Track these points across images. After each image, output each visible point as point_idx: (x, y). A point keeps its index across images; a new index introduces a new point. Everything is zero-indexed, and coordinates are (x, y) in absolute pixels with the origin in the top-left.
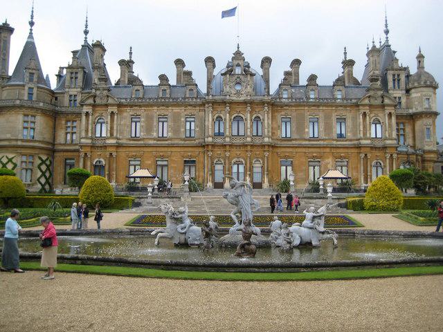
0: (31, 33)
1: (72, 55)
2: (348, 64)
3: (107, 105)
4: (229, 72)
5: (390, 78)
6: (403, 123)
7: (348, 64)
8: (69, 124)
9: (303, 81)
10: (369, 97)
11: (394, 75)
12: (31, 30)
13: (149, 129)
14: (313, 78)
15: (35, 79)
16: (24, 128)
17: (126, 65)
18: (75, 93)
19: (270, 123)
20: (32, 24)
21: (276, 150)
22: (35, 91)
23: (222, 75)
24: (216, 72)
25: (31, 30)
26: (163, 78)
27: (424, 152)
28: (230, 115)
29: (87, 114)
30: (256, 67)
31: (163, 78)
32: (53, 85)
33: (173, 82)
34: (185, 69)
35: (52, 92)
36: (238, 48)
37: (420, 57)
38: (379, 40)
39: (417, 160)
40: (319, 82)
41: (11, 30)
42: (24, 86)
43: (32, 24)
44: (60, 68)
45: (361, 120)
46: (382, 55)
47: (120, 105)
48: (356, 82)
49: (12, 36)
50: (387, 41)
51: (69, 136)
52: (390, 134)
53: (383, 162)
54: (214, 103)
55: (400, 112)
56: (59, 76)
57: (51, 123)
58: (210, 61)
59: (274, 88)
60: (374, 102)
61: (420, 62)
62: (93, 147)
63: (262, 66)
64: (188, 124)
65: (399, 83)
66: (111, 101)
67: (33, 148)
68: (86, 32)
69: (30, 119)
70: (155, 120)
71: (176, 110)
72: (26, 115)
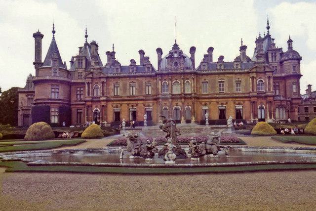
0: (54, 38)
1: (79, 49)
2: (243, 48)
3: (100, 78)
4: (171, 56)
5: (270, 56)
6: (278, 82)
7: (243, 48)
8: (79, 89)
9: (215, 59)
10: (256, 67)
11: (272, 53)
12: (54, 36)
13: (125, 89)
14: (221, 58)
16: (52, 92)
17: (111, 55)
18: (81, 71)
19: (195, 85)
20: (54, 32)
21: (199, 100)
23: (166, 58)
24: (163, 56)
25: (54, 36)
26: (133, 61)
27: (292, 99)
28: (172, 82)
29: (88, 83)
30: (187, 53)
31: (133, 61)
32: (69, 67)
33: (138, 63)
34: (144, 56)
35: (68, 72)
37: (290, 42)
38: (263, 33)
39: (287, 104)
40: (225, 60)
41: (42, 36)
42: (51, 68)
43: (54, 32)
44: (72, 57)
45: (251, 81)
46: (265, 42)
47: (107, 78)
48: (249, 59)
49: (42, 39)
50: (268, 33)
51: (79, 96)
52: (269, 90)
53: (265, 105)
54: (161, 74)
55: (276, 75)
56: (72, 62)
57: (67, 89)
58: (159, 51)
59: (197, 65)
60: (258, 70)
61: (289, 44)
62: (92, 101)
63: (190, 52)
64: (147, 87)
65: (275, 58)
66: (102, 75)
68: (86, 36)
69: (55, 87)
70: (128, 85)
71: (140, 79)
72: (52, 85)
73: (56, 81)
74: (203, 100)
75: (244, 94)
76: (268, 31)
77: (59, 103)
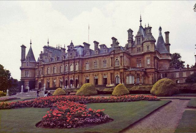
0: (31, 47)
20: (31, 44)
22: (29, 63)
27: (146, 69)
71: (58, 64)
72: (26, 71)
73: (27, 68)
74: (86, 74)
75: (108, 68)
76: (141, 23)
77: (28, 79)
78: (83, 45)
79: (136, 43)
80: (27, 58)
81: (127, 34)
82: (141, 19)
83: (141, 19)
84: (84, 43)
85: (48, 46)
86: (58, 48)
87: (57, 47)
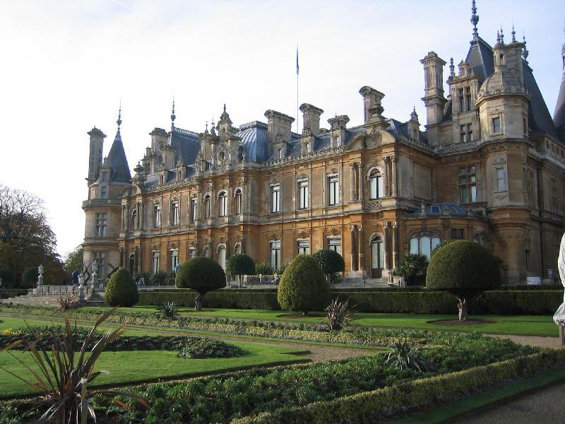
0: (119, 132)
12: (119, 129)
15: (108, 178)
25: (119, 129)
36: (225, 109)
43: (119, 122)
67: (102, 244)
78: (265, 120)
79: (456, 106)
80: (108, 170)
81: (420, 70)
82: (475, 12)
83: (475, 12)
84: (268, 114)
85: (173, 127)
86: (210, 133)
87: (207, 131)
